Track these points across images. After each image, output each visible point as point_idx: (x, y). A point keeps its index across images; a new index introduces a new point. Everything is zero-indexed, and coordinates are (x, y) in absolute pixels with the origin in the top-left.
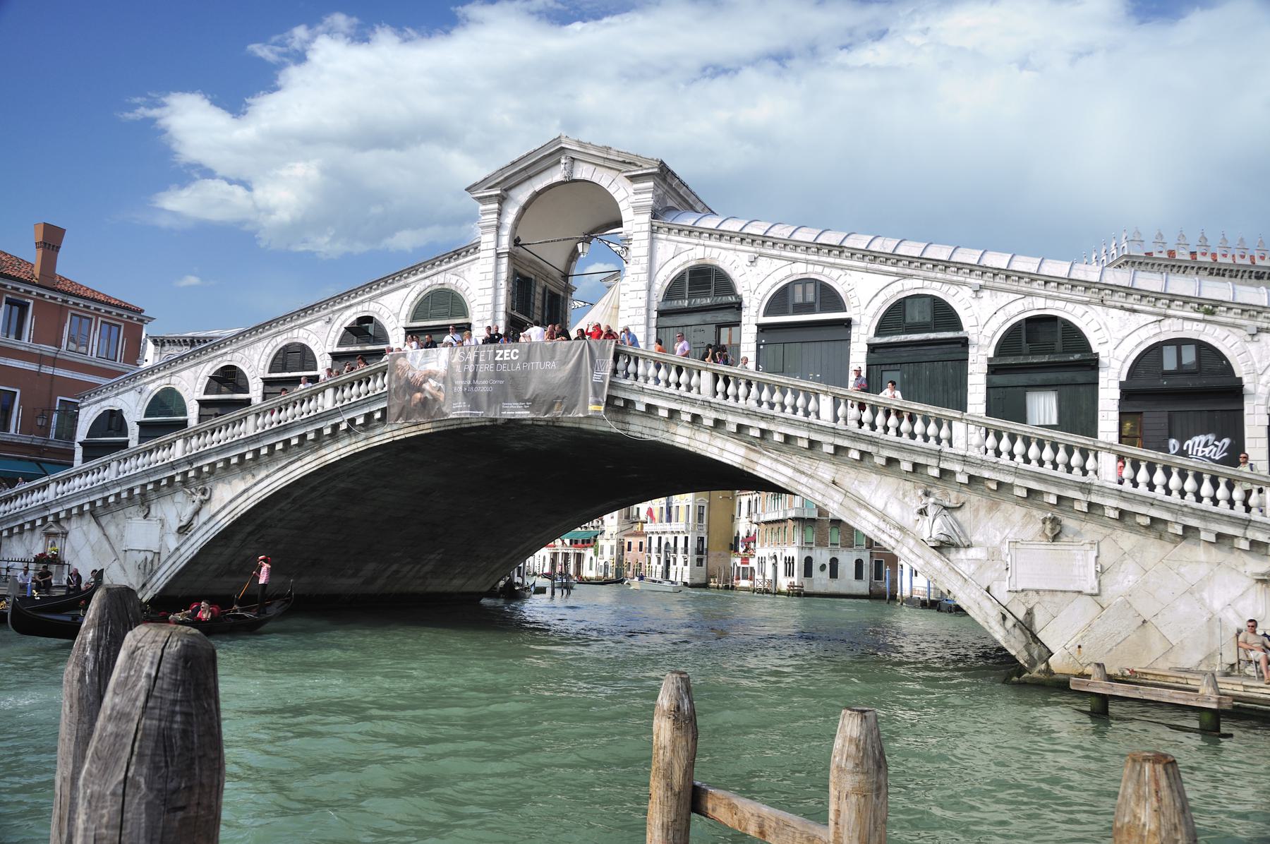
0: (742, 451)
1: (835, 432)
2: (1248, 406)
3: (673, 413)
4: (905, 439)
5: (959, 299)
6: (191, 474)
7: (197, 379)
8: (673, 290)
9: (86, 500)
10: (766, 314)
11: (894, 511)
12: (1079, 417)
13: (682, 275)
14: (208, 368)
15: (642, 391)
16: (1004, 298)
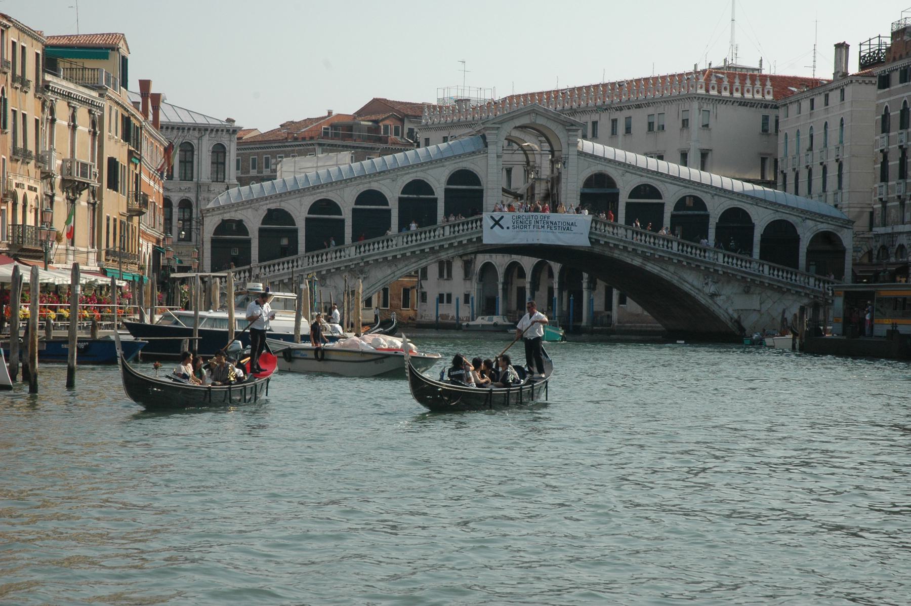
0: (641, 260)
1: (680, 255)
2: (801, 243)
3: (616, 246)
4: (702, 258)
5: (706, 198)
6: (362, 264)
7: (301, 205)
8: (589, 183)
9: (287, 277)
10: (630, 197)
11: (696, 283)
12: (746, 247)
13: (591, 176)
14: (309, 201)
15: (605, 236)
16: (723, 200)
